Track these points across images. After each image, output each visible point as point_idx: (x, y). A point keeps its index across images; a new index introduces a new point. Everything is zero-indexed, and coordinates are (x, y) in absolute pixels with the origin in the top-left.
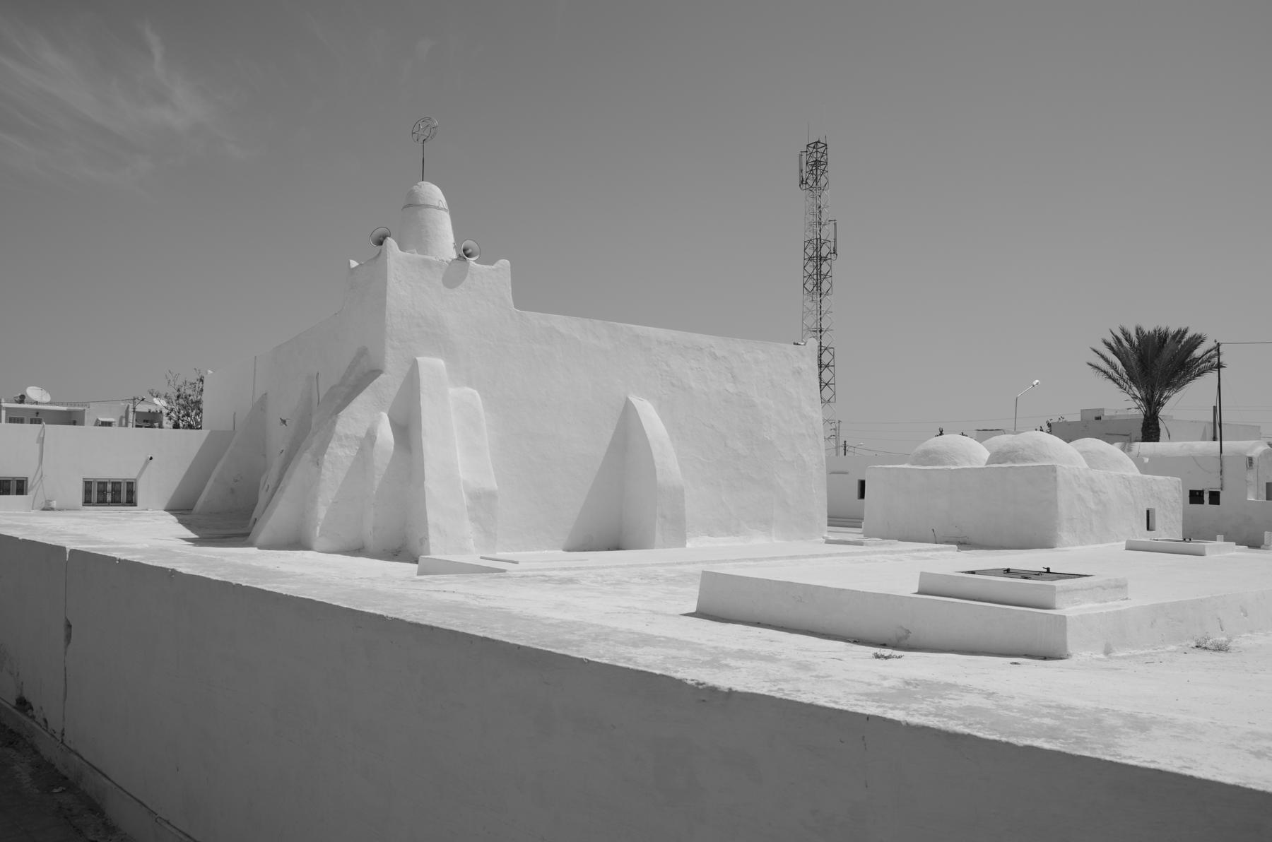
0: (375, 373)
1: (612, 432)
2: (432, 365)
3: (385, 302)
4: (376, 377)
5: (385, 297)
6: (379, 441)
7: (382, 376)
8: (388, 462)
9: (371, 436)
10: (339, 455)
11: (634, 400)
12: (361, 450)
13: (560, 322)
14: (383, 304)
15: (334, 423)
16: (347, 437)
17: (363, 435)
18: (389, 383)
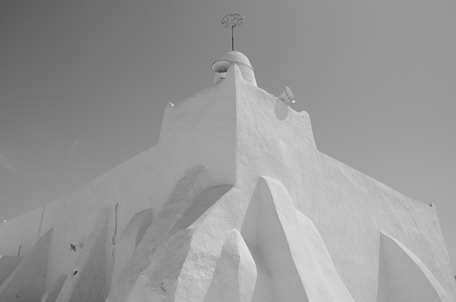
1: (378, 259)
2: (275, 185)
3: (236, 116)
4: (227, 191)
5: (236, 113)
6: (242, 262)
7: (234, 189)
8: (253, 287)
9: (230, 257)
10: (195, 277)
12: (217, 272)
13: (340, 166)
14: (235, 118)
15: (189, 239)
16: (202, 255)
17: (218, 253)
18: (239, 198)
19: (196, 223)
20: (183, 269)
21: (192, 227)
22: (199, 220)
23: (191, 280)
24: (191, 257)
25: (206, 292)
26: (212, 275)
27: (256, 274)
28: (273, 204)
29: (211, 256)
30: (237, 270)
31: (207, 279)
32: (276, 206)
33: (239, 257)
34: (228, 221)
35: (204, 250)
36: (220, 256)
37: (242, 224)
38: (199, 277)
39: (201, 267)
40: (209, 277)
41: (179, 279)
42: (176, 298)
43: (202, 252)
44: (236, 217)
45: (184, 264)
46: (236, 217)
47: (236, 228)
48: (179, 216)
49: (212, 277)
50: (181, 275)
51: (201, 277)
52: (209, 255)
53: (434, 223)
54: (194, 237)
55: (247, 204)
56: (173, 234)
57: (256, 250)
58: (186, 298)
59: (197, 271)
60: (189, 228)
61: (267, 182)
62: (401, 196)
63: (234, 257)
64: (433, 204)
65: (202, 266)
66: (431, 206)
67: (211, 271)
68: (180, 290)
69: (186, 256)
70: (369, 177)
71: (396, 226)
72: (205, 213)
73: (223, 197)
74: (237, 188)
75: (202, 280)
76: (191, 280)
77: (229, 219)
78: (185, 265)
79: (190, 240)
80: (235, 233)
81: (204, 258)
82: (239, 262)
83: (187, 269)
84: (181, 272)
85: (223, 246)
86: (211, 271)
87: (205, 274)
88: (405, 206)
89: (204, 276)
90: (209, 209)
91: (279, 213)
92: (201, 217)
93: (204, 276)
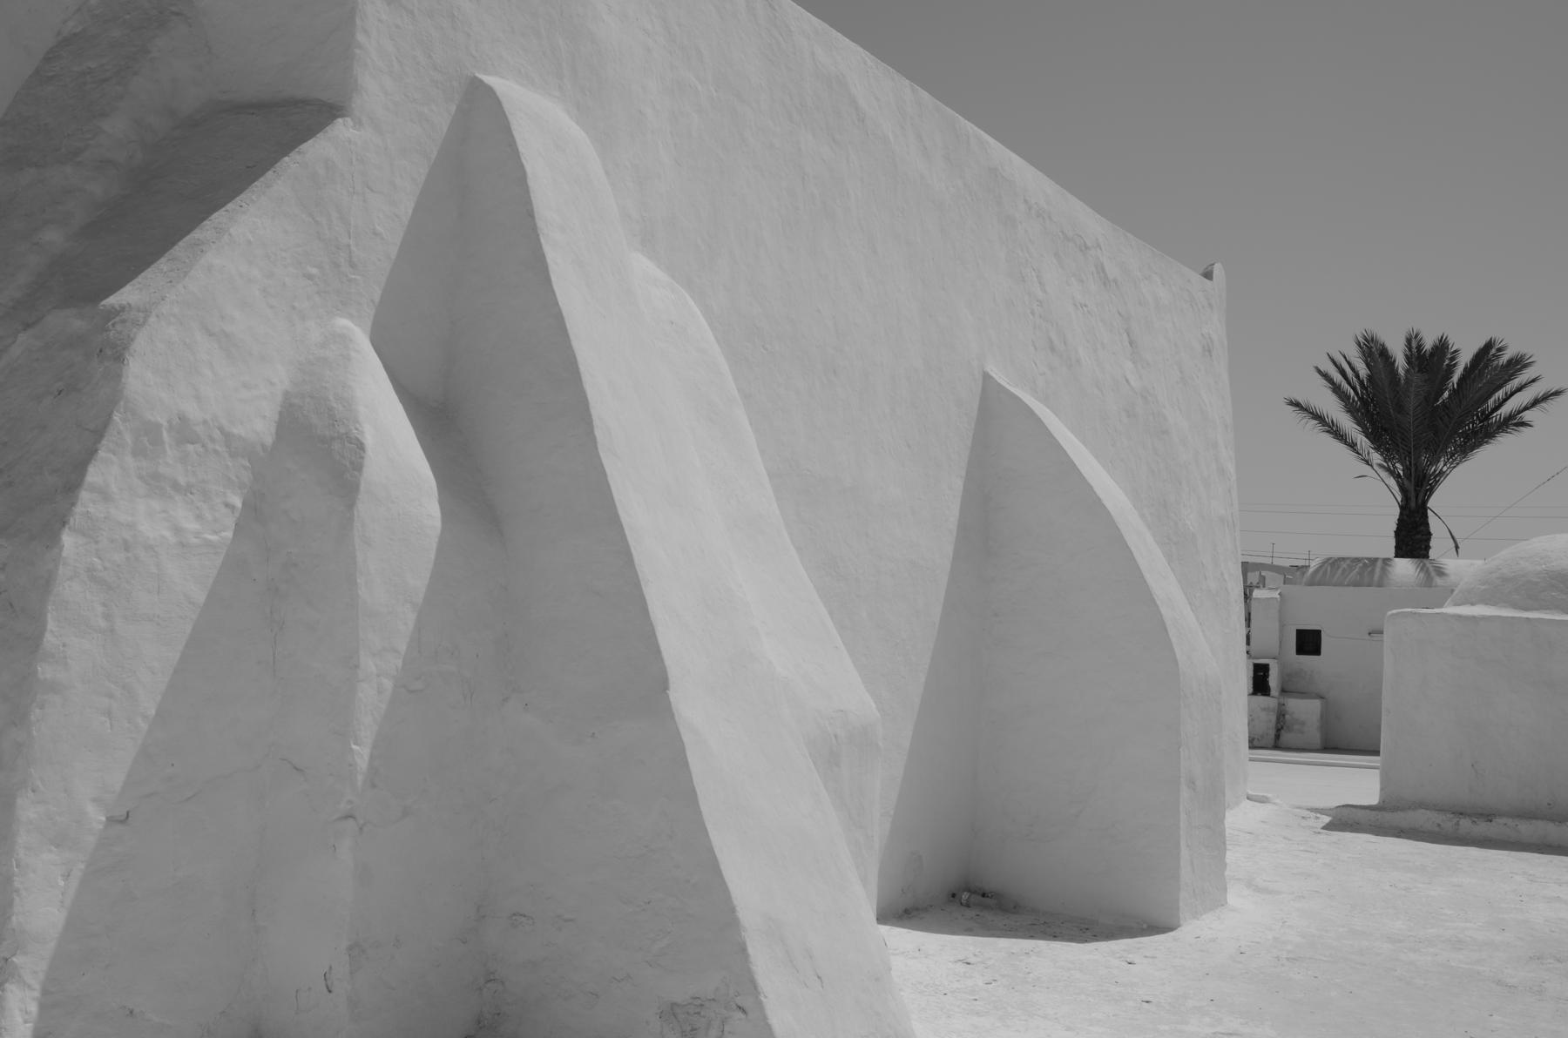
0: (286, 118)
1: (959, 484)
6: (375, 469)
7: (341, 129)
8: (418, 581)
9: (315, 444)
11: (1002, 380)
12: (255, 512)
13: (849, 59)
16: (184, 432)
17: (259, 425)
19: (153, 277)
20: (84, 495)
21: (128, 296)
22: (163, 264)
23: (127, 547)
24: (128, 438)
25: (201, 597)
26: (230, 522)
27: (438, 523)
28: (531, 214)
29: (228, 437)
30: (351, 506)
31: (208, 544)
32: (540, 224)
33: (361, 446)
34: (310, 277)
35: (192, 410)
36: (269, 440)
37: (377, 298)
38: (167, 534)
39: (176, 486)
40: (215, 532)
41: (68, 540)
42: (51, 625)
43: (183, 418)
44: (352, 265)
45: (91, 469)
46: (352, 265)
47: (351, 317)
48: (53, 237)
49: (229, 534)
50: (76, 519)
51: (177, 530)
52: (217, 434)
53: (1208, 350)
54: (141, 342)
55: (406, 207)
56: (27, 326)
57: (439, 417)
58: (103, 624)
59: (156, 505)
60: (113, 300)
61: (506, 106)
62: (1093, 225)
63: (336, 446)
64: (1218, 270)
65: (182, 480)
66: (1208, 275)
67: (227, 505)
68: (71, 590)
69: (99, 434)
70: (970, 127)
71: (1053, 349)
72: (196, 234)
73: (290, 163)
74: (358, 124)
75: (182, 545)
76: (127, 547)
77: (314, 271)
78: (93, 475)
79: (119, 359)
80: (344, 339)
81: (190, 447)
82: (359, 467)
83: (105, 495)
84: (78, 509)
85: (286, 394)
86: (227, 505)
87: (199, 517)
88: (1101, 269)
89: (191, 525)
90: (219, 217)
91: (551, 255)
92: (179, 250)
93: (191, 525)
